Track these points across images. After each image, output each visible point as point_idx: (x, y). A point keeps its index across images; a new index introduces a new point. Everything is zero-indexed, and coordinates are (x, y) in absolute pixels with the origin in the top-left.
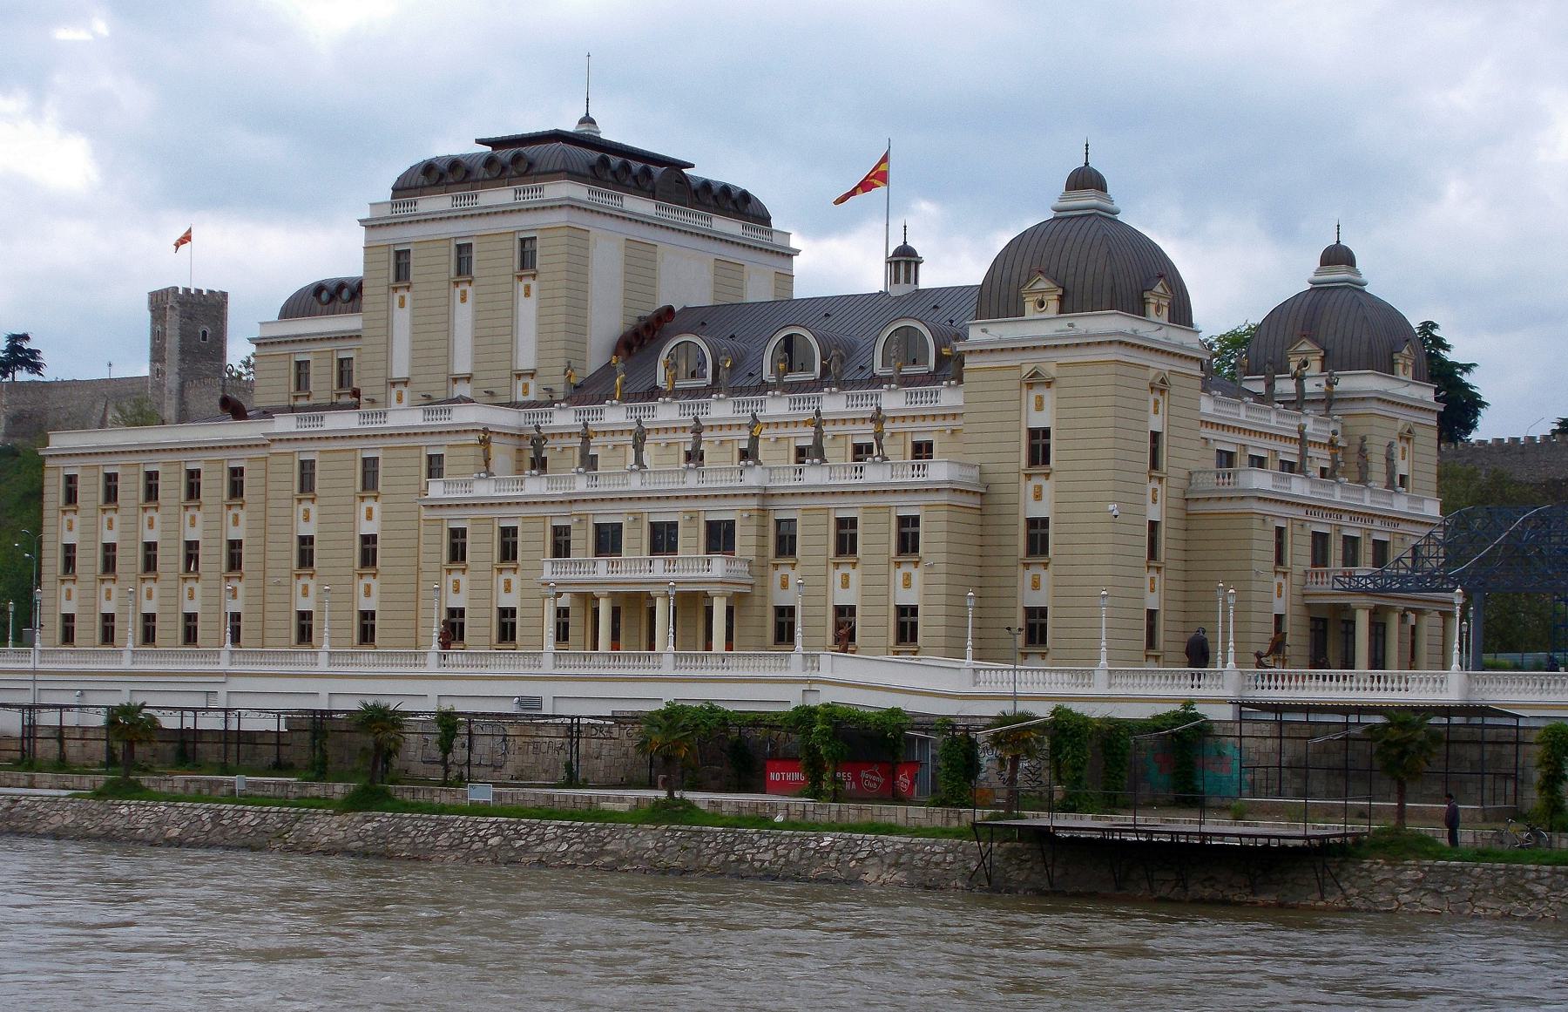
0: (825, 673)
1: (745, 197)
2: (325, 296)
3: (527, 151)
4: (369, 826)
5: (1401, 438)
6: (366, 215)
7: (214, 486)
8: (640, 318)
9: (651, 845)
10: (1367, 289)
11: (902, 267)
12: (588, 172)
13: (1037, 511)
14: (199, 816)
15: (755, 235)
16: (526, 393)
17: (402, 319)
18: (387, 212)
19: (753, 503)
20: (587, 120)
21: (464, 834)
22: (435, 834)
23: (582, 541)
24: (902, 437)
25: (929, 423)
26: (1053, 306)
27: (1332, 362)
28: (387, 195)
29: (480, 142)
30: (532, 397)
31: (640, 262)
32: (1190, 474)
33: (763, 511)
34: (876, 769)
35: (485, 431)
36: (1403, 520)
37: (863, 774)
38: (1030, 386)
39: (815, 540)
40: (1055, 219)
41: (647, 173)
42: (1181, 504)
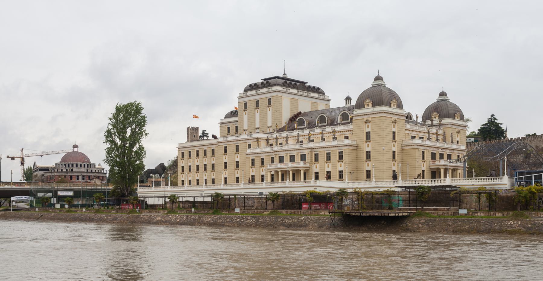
0: (318, 185)
1: (319, 89)
2: (233, 113)
3: (269, 81)
4: (215, 218)
5: (457, 133)
6: (239, 96)
7: (209, 153)
8: (294, 114)
9: (268, 220)
10: (450, 101)
11: (347, 101)
12: (282, 84)
13: (368, 149)
14: (184, 217)
15: (320, 97)
16: (270, 131)
17: (246, 117)
18: (242, 95)
19: (309, 150)
20: (285, 74)
21: (232, 219)
22: (227, 219)
23: (277, 160)
24: (342, 135)
25: (348, 132)
26: (370, 105)
27: (441, 116)
28: (243, 91)
29: (261, 80)
30: (271, 132)
31: (294, 103)
32: (403, 141)
33: (312, 152)
34: (324, 204)
35: (258, 138)
36: (455, 150)
37: (321, 205)
38: (366, 123)
39: (322, 157)
40: (372, 87)
41: (296, 84)
42: (401, 147)
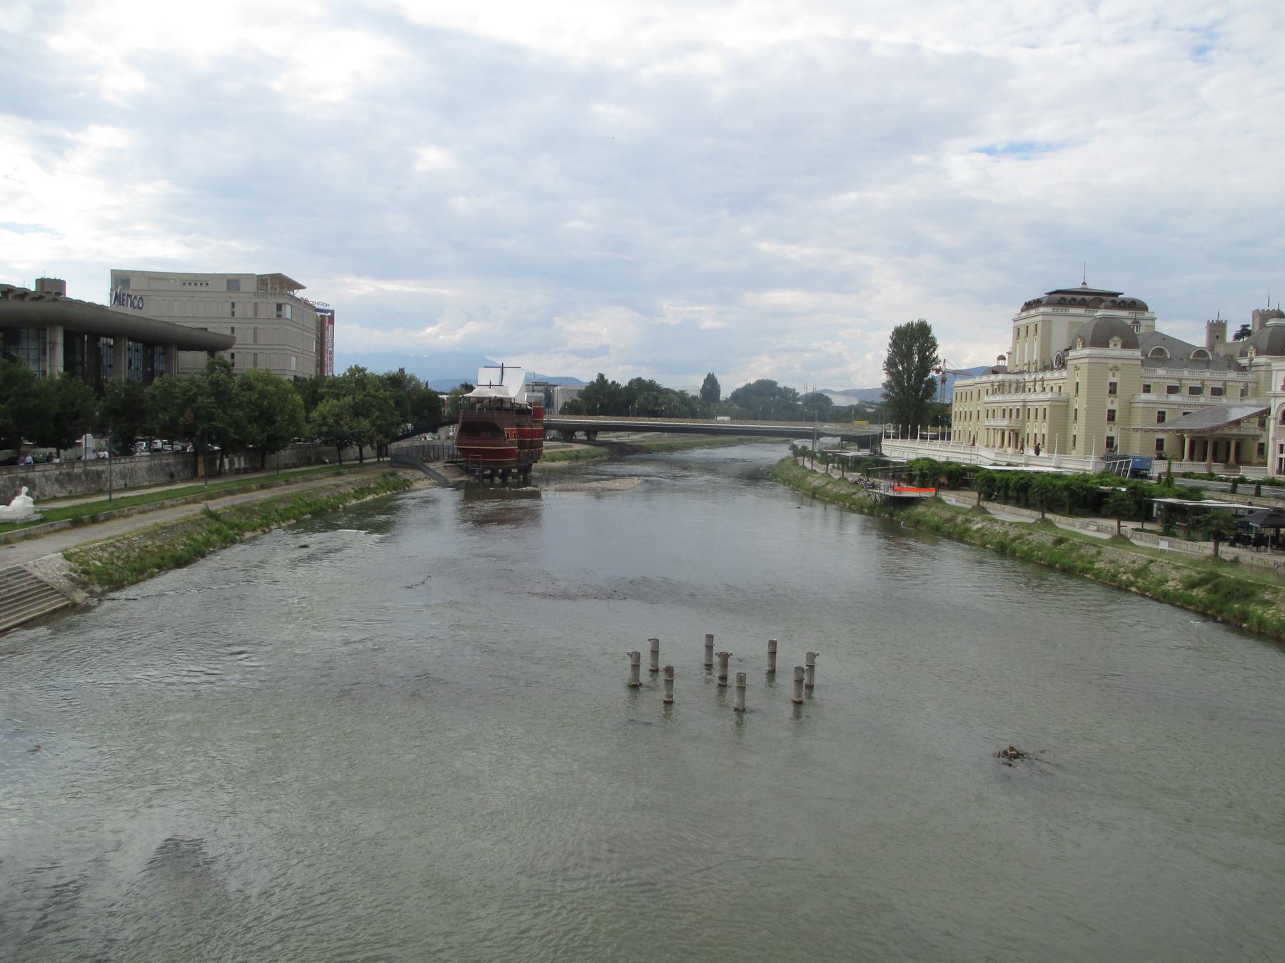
19: (1021, 404)
20: (1084, 283)
